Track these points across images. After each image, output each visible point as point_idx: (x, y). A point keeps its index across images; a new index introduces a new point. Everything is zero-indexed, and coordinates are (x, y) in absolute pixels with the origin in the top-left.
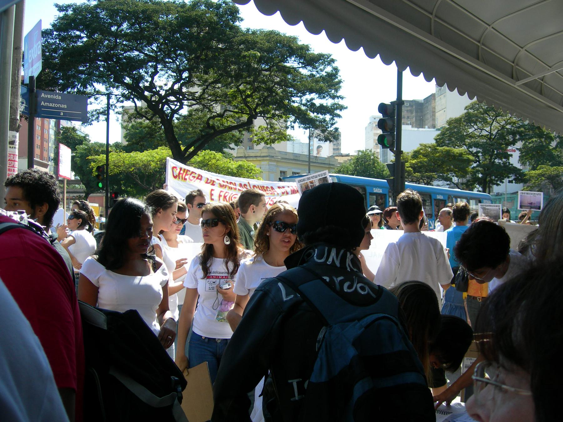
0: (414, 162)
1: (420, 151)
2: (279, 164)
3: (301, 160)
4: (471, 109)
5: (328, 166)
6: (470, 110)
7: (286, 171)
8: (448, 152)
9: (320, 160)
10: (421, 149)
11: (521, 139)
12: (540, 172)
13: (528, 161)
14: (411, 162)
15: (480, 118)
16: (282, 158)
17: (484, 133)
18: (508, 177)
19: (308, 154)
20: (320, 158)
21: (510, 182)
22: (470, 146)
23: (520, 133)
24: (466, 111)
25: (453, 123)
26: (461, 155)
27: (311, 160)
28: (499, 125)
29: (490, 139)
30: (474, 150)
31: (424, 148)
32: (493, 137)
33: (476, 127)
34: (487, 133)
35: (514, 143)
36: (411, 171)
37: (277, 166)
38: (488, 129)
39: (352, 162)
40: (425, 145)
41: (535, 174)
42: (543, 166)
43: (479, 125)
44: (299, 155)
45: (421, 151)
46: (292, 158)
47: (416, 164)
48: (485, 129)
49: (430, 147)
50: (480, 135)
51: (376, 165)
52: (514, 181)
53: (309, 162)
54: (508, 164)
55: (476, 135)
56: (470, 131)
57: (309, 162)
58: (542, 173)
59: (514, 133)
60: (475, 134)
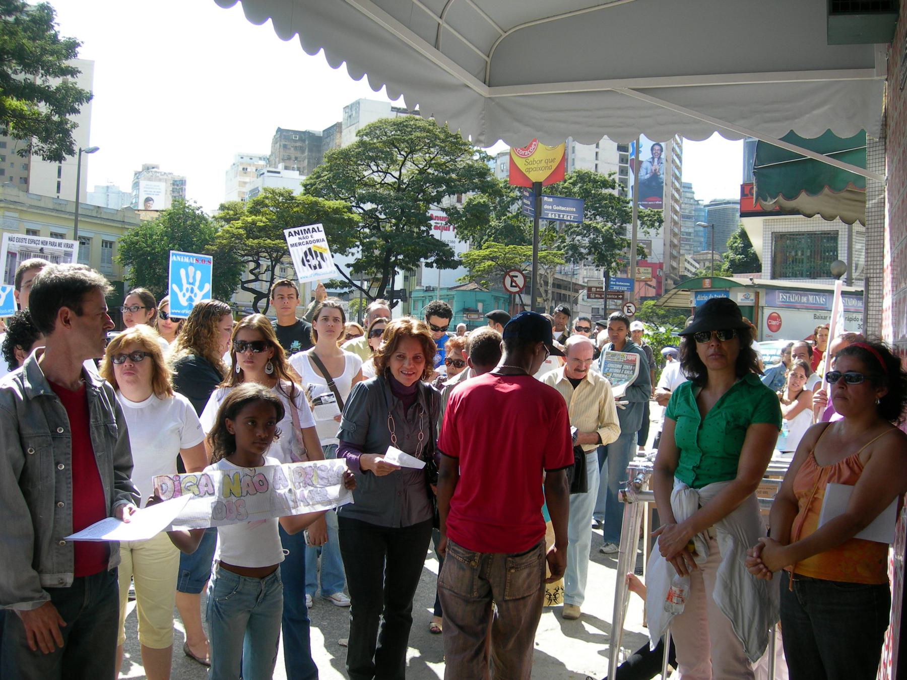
0: (249, 219)
1: (263, 202)
2: (24, 216)
3: (68, 211)
4: (366, 136)
5: (120, 226)
6: (365, 137)
7: (39, 231)
8: (316, 203)
9: (105, 212)
10: (267, 198)
11: (451, 192)
12: (487, 253)
13: (472, 235)
14: (244, 219)
15: (382, 152)
16: (31, 206)
17: (389, 180)
18: (426, 258)
19: (75, 201)
20: (105, 210)
21: (429, 265)
22: (363, 199)
23: (448, 182)
24: (358, 139)
25: (336, 159)
26: (336, 211)
27: (80, 212)
28: (417, 168)
29: (399, 189)
30: (368, 206)
31: (270, 195)
32: (404, 186)
33: (375, 168)
34: (394, 180)
35: (438, 199)
36: (241, 235)
37: (20, 220)
38: (397, 174)
39: (162, 219)
40: (273, 190)
41: (478, 256)
42: (493, 243)
43: (384, 166)
44: (65, 203)
45: (267, 201)
46: (51, 206)
47: (254, 223)
48: (393, 173)
49: (281, 195)
50: (383, 182)
51: (202, 226)
52: (435, 265)
53: (77, 214)
54: (425, 234)
55: (376, 182)
56: (366, 173)
57: (77, 214)
58: (490, 254)
59: (437, 182)
60: (374, 181)
